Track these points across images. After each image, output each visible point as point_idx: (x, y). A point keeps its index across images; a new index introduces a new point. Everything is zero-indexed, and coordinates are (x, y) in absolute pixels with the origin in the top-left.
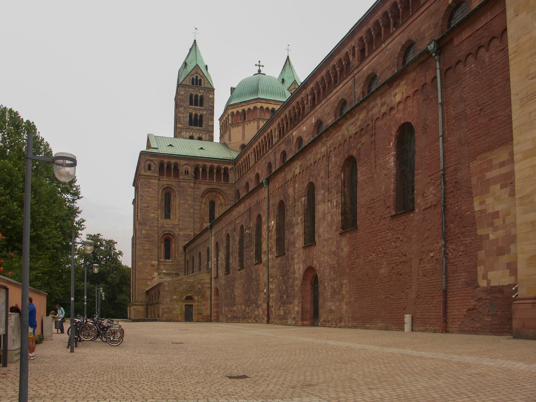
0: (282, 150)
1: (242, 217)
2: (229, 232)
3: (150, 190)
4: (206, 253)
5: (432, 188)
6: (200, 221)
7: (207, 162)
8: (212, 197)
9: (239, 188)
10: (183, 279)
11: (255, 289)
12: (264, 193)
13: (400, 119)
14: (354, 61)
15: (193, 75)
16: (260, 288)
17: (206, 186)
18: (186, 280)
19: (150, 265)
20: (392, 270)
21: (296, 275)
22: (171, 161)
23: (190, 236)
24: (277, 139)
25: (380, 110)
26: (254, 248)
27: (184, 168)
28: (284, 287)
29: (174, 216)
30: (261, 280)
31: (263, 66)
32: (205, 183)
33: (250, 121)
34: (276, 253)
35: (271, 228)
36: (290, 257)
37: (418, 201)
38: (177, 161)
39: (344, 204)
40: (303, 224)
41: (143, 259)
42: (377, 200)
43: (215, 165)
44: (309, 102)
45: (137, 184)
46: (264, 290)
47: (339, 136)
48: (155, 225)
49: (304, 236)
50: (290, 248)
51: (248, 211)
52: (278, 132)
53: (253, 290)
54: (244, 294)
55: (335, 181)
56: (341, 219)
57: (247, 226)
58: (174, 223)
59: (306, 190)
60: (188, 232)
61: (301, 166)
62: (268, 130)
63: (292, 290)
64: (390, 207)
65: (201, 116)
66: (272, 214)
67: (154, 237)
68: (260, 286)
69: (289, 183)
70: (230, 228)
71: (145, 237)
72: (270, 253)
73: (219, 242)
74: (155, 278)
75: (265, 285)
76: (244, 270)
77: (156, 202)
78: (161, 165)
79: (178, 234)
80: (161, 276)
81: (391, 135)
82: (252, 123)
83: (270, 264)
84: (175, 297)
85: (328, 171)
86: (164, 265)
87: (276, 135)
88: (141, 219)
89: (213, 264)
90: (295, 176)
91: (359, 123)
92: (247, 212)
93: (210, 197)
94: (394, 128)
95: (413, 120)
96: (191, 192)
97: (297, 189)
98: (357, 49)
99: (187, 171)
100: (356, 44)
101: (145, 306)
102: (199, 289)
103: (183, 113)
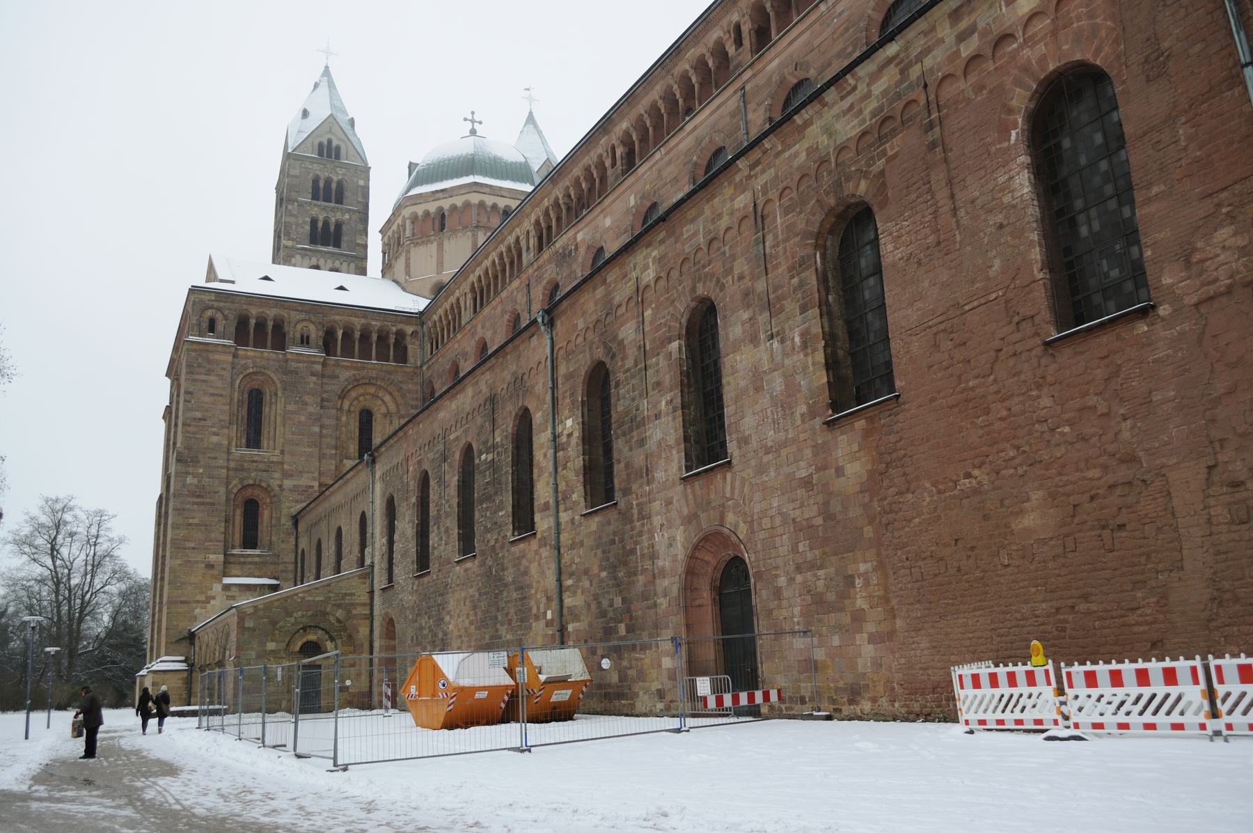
0: (547, 277)
1: (467, 423)
2: (426, 466)
3: (212, 378)
4: (356, 527)
5: (1224, 233)
6: (336, 454)
8: (367, 397)
9: (431, 375)
10: (297, 594)
11: (512, 611)
12: (539, 348)
13: (1043, 59)
14: (739, 55)
15: (321, 136)
16: (530, 609)
18: (303, 598)
19: (203, 565)
20: (1073, 516)
21: (660, 563)
22: (268, 312)
23: (310, 490)
24: (532, 254)
25: (958, 53)
26: (508, 499)
28: (618, 601)
29: (271, 442)
30: (534, 584)
31: (480, 123)
33: (454, 231)
34: (583, 504)
35: (564, 439)
36: (635, 511)
37: (1167, 280)
38: (282, 313)
39: (830, 339)
40: (680, 412)
41: (185, 548)
42: (976, 303)
44: (619, 162)
45: (177, 367)
46: (545, 613)
47: (796, 155)
48: (221, 462)
49: (683, 446)
50: (634, 487)
51: (488, 403)
52: (536, 238)
53: (507, 614)
54: (478, 628)
55: (792, 277)
56: (825, 380)
57: (485, 443)
58: (271, 459)
59: (684, 321)
60: (304, 481)
61: (660, 260)
62: (509, 237)
63: (648, 608)
64: (1032, 317)
65: (339, 226)
66: (568, 400)
67: (218, 492)
68: (533, 603)
69: (623, 309)
70: (431, 456)
71: (193, 494)
72: (562, 507)
73: (395, 496)
75: (549, 599)
76: (476, 562)
78: (242, 322)
79: (280, 486)
80: (230, 594)
81: (1010, 111)
83: (564, 537)
84: (271, 646)
85: (765, 255)
87: (531, 246)
88: (185, 448)
89: (377, 553)
90: (640, 291)
91: (872, 105)
92: (482, 408)
94: (1018, 90)
95: (1098, 51)
96: (315, 383)
97: (651, 323)
98: (746, 28)
99: (305, 336)
100: (744, 15)
102: (338, 621)
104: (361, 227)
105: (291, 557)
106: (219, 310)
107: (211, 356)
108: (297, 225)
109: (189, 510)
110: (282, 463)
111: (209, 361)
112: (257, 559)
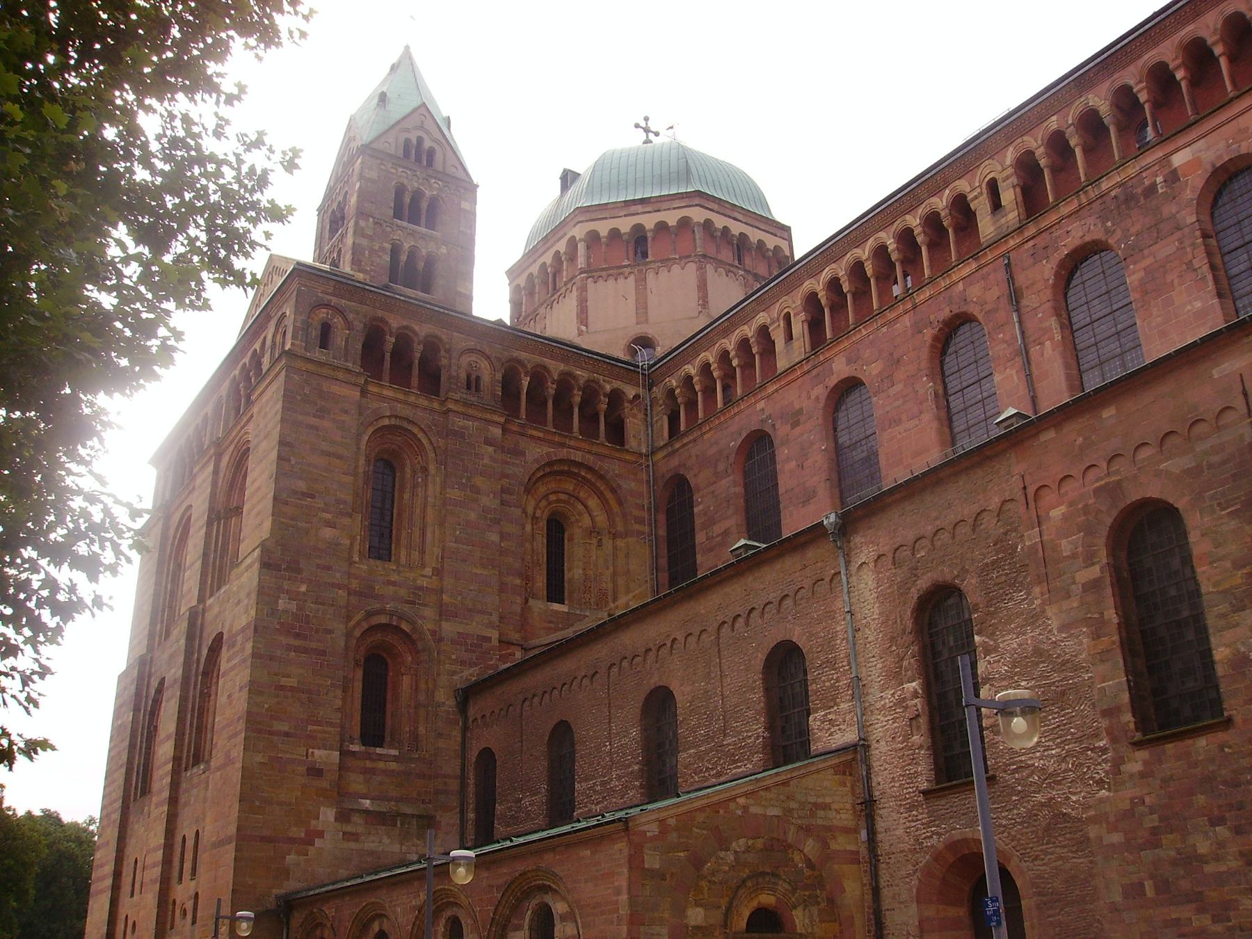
3: (326, 424)
7: (552, 358)
8: (562, 497)
17: (546, 449)
19: (302, 769)
22: (416, 328)
27: (465, 360)
32: (541, 435)
33: (666, 262)
41: (271, 733)
43: (580, 373)
48: (338, 577)
60: (476, 627)
67: (330, 632)
74: (321, 834)
77: (349, 479)
82: (676, 269)
86: (365, 771)
105: (451, 767)
106: (339, 311)
108: (372, 251)
112: (393, 765)
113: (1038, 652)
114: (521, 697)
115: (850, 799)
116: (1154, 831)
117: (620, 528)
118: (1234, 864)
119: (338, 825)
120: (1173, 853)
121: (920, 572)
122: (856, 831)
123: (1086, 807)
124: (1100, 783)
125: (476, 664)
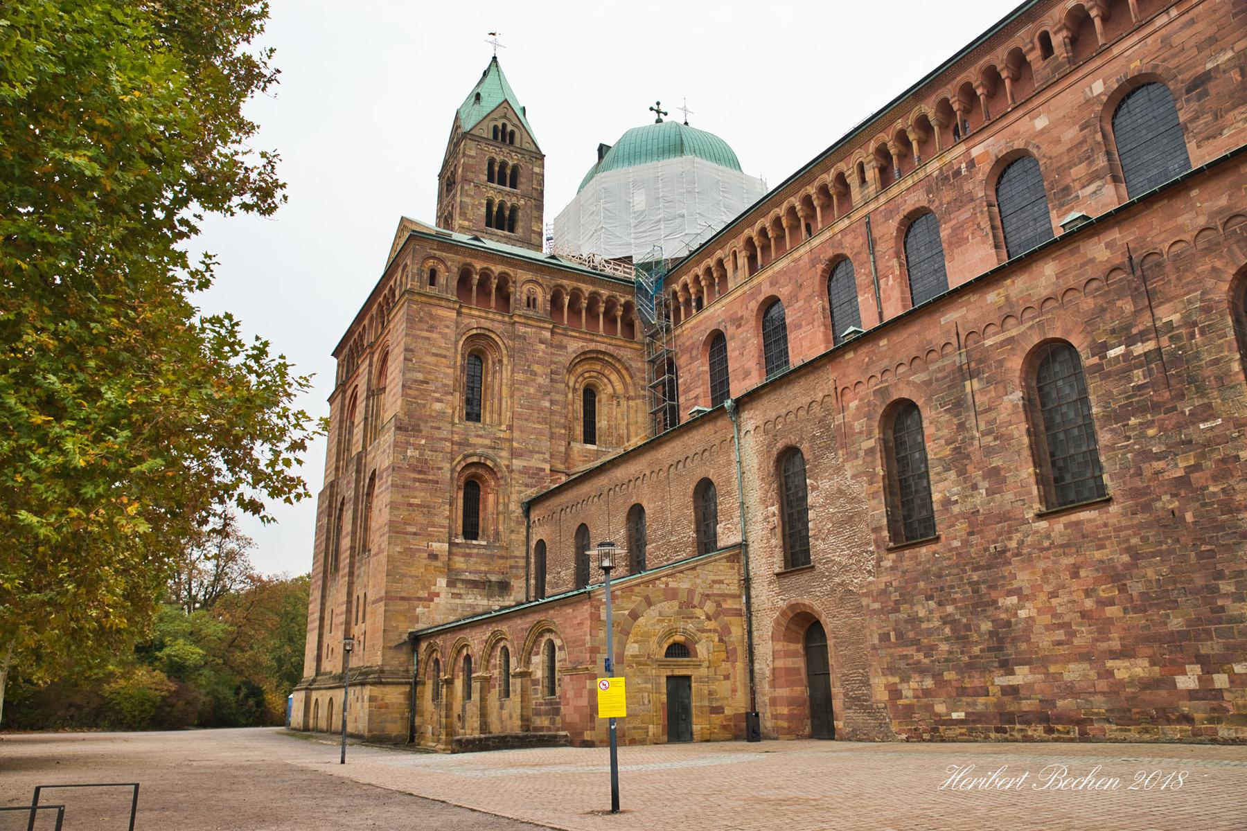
3: (435, 335)
7: (584, 282)
8: (593, 374)
17: (581, 344)
19: (426, 555)
22: (493, 268)
23: (542, 474)
27: (525, 288)
29: (496, 416)
41: (406, 533)
48: (445, 434)
60: (534, 462)
65: (514, 210)
67: (440, 469)
71: (413, 469)
74: (438, 595)
77: (451, 371)
93: (587, 375)
96: (543, 352)
101: (407, 688)
103: (472, 197)
104: (535, 214)
105: (521, 551)
106: (440, 260)
107: (434, 311)
109: (409, 487)
110: (511, 440)
111: (432, 317)
113: (840, 491)
114: (560, 508)
115: (737, 577)
116: (896, 602)
117: (632, 394)
118: (937, 624)
119: (448, 589)
120: (906, 616)
121: (778, 438)
122: (740, 596)
123: (862, 587)
124: (869, 572)
125: (535, 486)
